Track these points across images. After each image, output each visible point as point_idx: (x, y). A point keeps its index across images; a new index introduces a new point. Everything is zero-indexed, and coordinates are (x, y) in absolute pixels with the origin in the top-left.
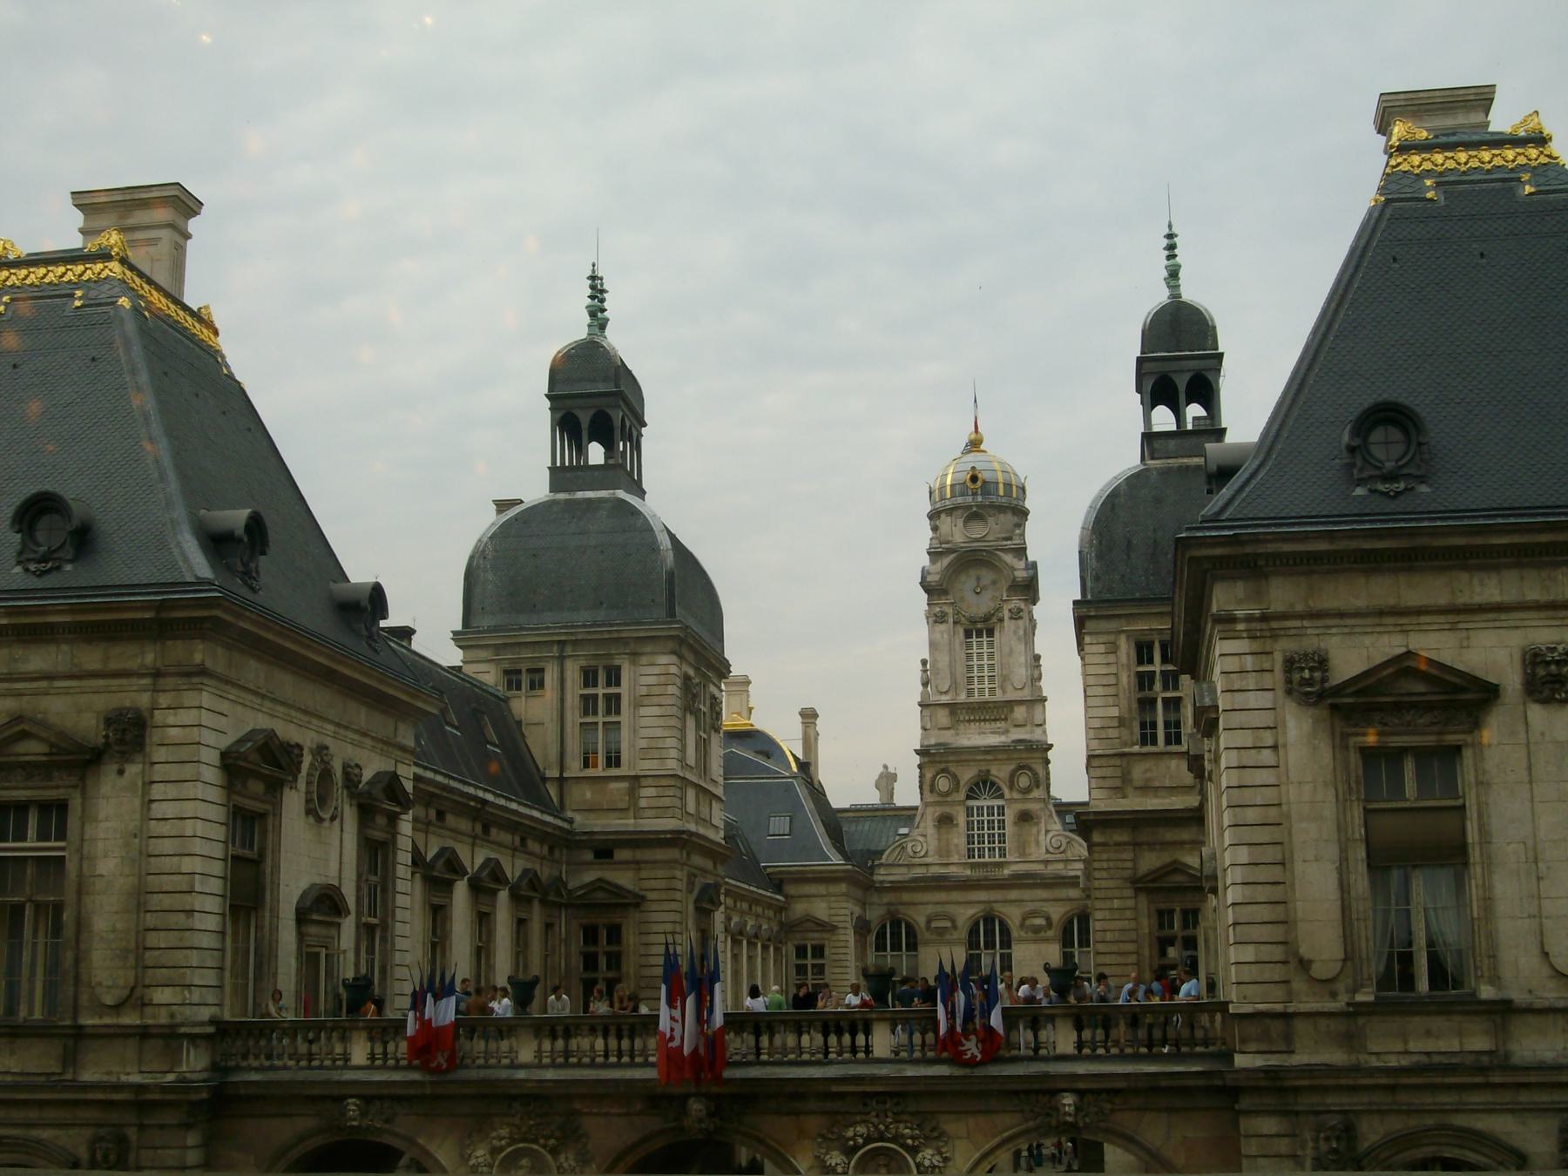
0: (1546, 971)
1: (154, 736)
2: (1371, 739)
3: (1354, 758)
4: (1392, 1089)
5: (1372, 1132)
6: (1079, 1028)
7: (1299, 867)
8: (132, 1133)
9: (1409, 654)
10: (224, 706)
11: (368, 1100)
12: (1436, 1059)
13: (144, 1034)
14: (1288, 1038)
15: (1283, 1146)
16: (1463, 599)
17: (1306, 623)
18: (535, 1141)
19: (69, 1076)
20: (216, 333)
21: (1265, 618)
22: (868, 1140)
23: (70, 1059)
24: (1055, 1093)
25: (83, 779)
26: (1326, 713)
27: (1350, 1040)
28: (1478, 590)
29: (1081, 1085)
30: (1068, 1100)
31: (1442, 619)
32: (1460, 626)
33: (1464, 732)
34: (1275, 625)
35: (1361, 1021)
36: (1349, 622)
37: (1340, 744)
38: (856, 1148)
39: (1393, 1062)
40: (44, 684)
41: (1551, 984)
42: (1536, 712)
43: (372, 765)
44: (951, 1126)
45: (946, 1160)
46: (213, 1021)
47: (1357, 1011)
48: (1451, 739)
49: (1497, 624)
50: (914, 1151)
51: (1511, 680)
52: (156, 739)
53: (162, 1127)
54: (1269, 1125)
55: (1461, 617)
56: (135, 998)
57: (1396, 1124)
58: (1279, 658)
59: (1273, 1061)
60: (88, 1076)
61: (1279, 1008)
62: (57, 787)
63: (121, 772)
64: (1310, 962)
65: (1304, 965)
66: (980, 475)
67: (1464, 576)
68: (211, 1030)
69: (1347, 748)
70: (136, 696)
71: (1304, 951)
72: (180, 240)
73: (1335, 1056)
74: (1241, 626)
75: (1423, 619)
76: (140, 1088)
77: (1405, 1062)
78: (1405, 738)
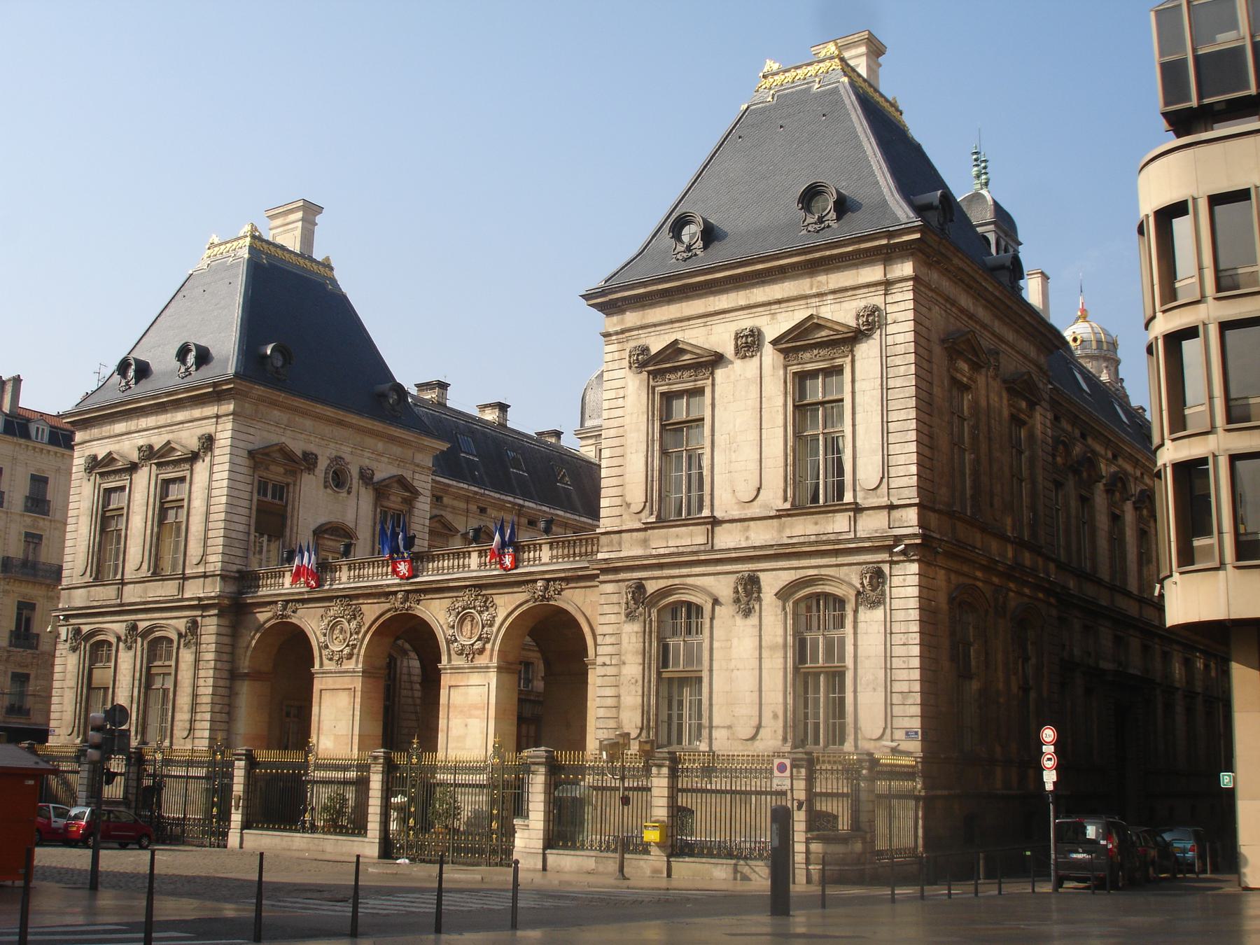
0: (734, 501)
1: (217, 444)
2: (665, 389)
3: (657, 398)
4: (661, 566)
5: (651, 587)
6: (551, 549)
7: (628, 456)
8: (199, 619)
9: (676, 342)
10: (252, 431)
11: (287, 602)
12: (681, 549)
13: (205, 576)
14: (620, 544)
15: (615, 598)
16: (711, 309)
17: (640, 332)
18: (343, 617)
19: (180, 597)
20: (332, 269)
21: (623, 332)
22: (464, 609)
23: (181, 589)
24: (535, 581)
25: (192, 466)
26: (645, 375)
27: (645, 542)
28: (717, 304)
29: (547, 576)
30: (540, 584)
31: (700, 321)
32: (708, 323)
33: (705, 379)
34: (627, 334)
35: (649, 532)
36: (658, 328)
37: (651, 390)
38: (459, 613)
39: (662, 551)
40: (181, 426)
41: (736, 507)
42: (738, 364)
43: (383, 471)
44: (499, 600)
45: (494, 617)
46: (239, 571)
47: (647, 527)
48: (700, 383)
49: (724, 320)
50: (480, 613)
51: (728, 350)
52: (216, 446)
53: (209, 616)
54: (609, 588)
55: (709, 319)
56: (203, 560)
57: (662, 584)
58: (628, 351)
59: (613, 555)
60: (186, 596)
61: (616, 529)
62: (183, 471)
63: (203, 461)
64: (630, 504)
65: (628, 505)
66: (1079, 337)
67: (711, 299)
68: (237, 575)
69: (653, 393)
70: (208, 428)
71: (628, 499)
72: (309, 226)
73: (639, 552)
74: (614, 338)
75: (691, 322)
76: (200, 599)
77: (667, 551)
78: (680, 385)
